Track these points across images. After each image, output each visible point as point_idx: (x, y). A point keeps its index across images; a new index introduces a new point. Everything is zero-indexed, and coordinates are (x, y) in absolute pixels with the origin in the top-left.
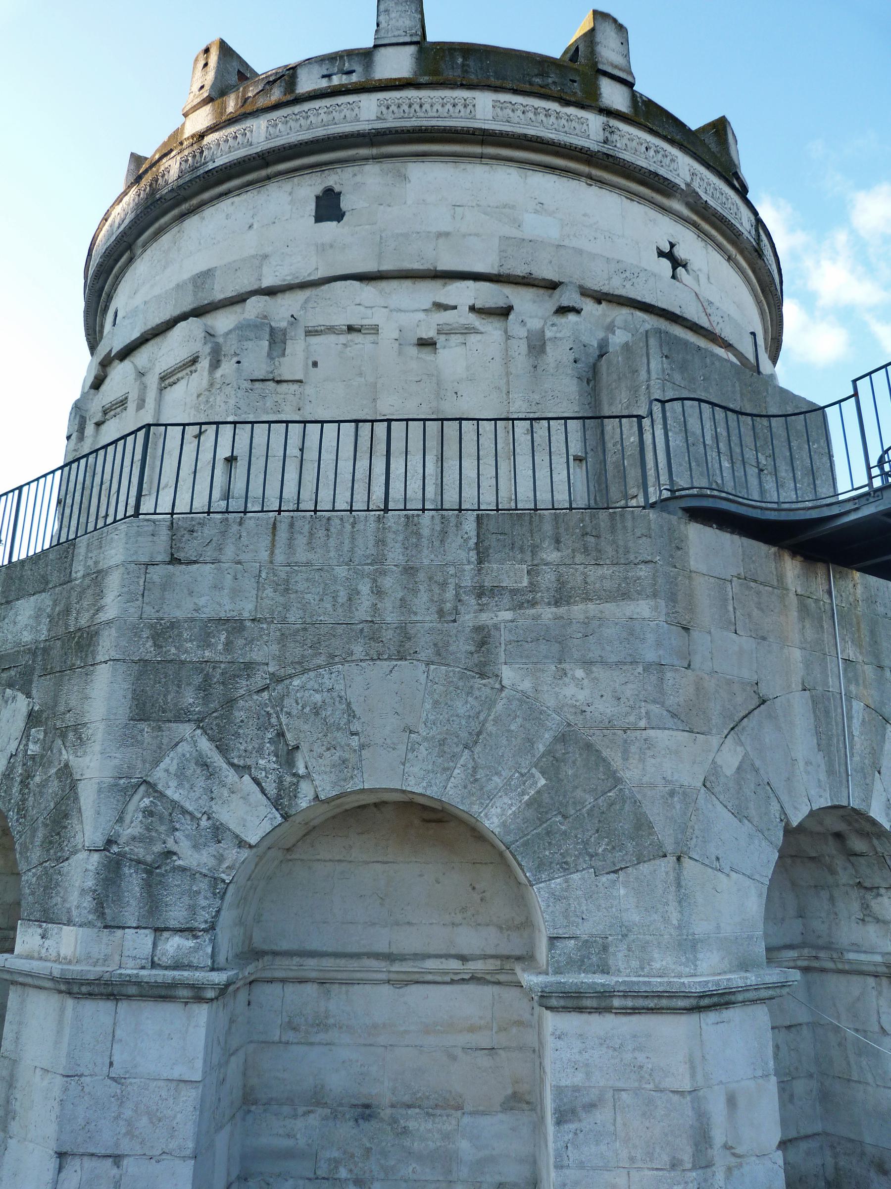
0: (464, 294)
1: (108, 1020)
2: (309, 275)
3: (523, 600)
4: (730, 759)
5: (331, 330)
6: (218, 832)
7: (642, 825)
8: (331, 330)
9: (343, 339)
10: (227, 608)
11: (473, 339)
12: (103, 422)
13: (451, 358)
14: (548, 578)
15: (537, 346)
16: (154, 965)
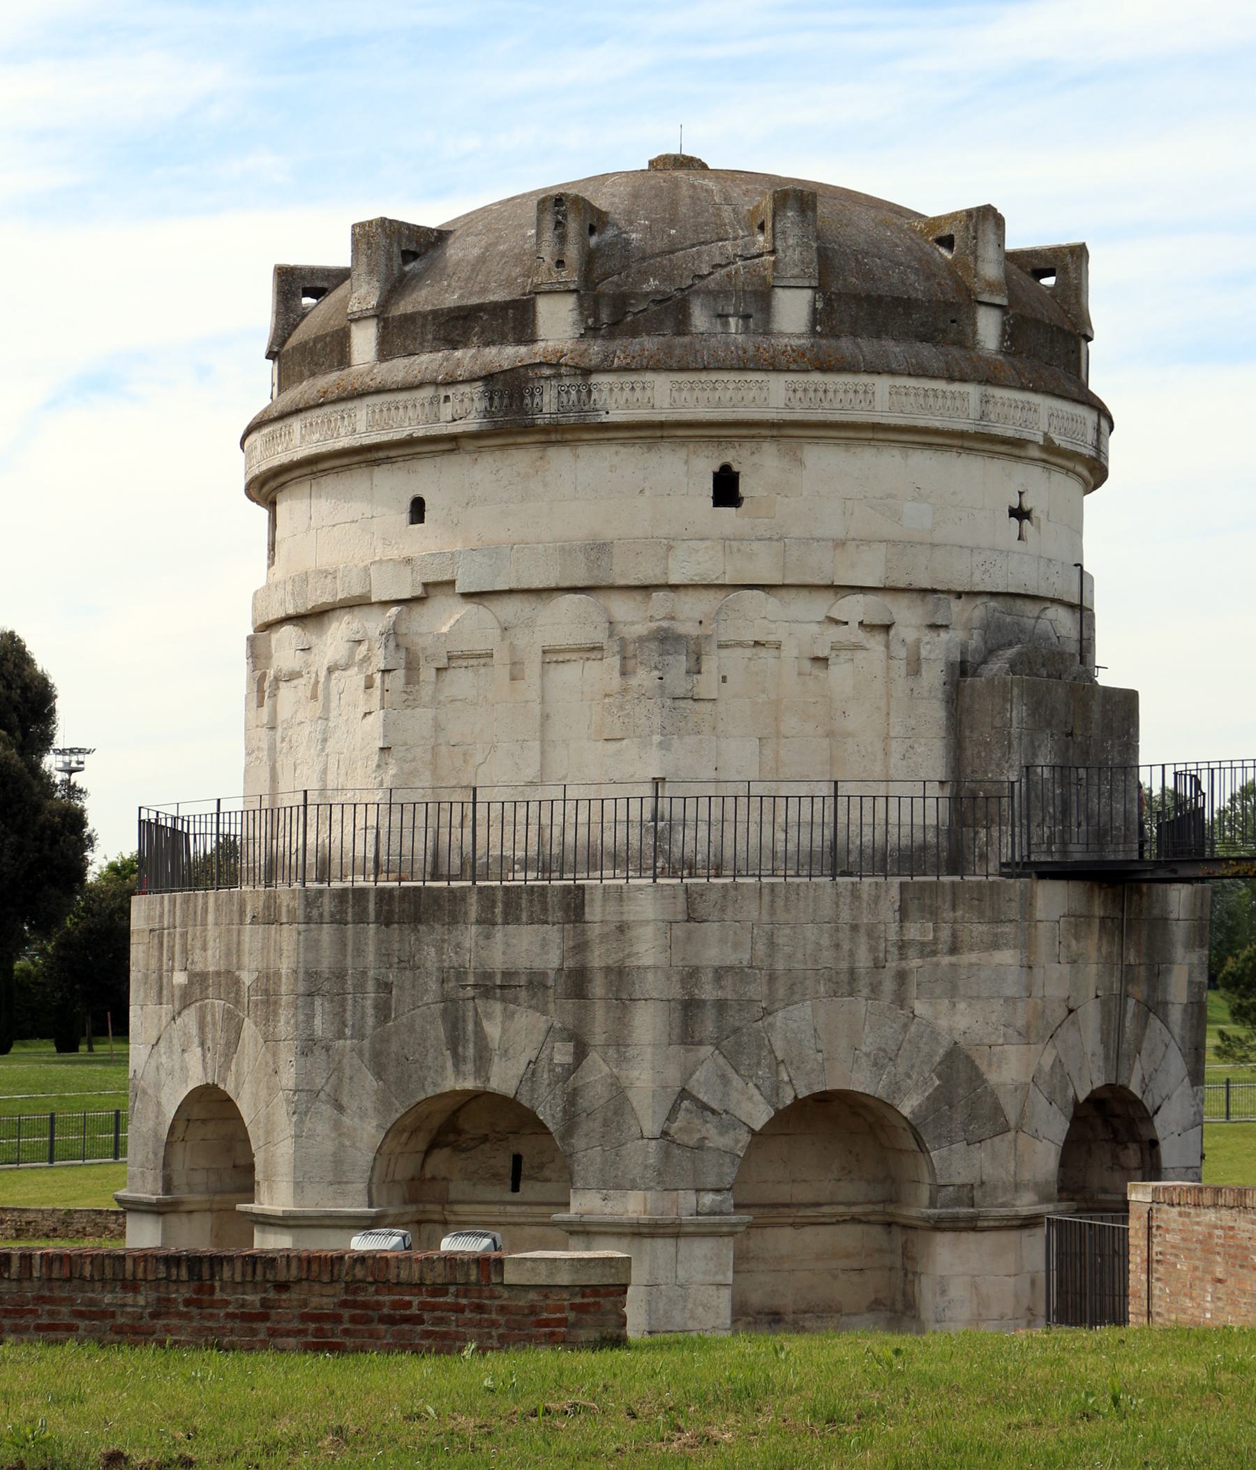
1: (673, 1250)
2: (717, 578)
5: (740, 644)
8: (740, 644)
9: (748, 652)
12: (446, 669)
16: (698, 1214)
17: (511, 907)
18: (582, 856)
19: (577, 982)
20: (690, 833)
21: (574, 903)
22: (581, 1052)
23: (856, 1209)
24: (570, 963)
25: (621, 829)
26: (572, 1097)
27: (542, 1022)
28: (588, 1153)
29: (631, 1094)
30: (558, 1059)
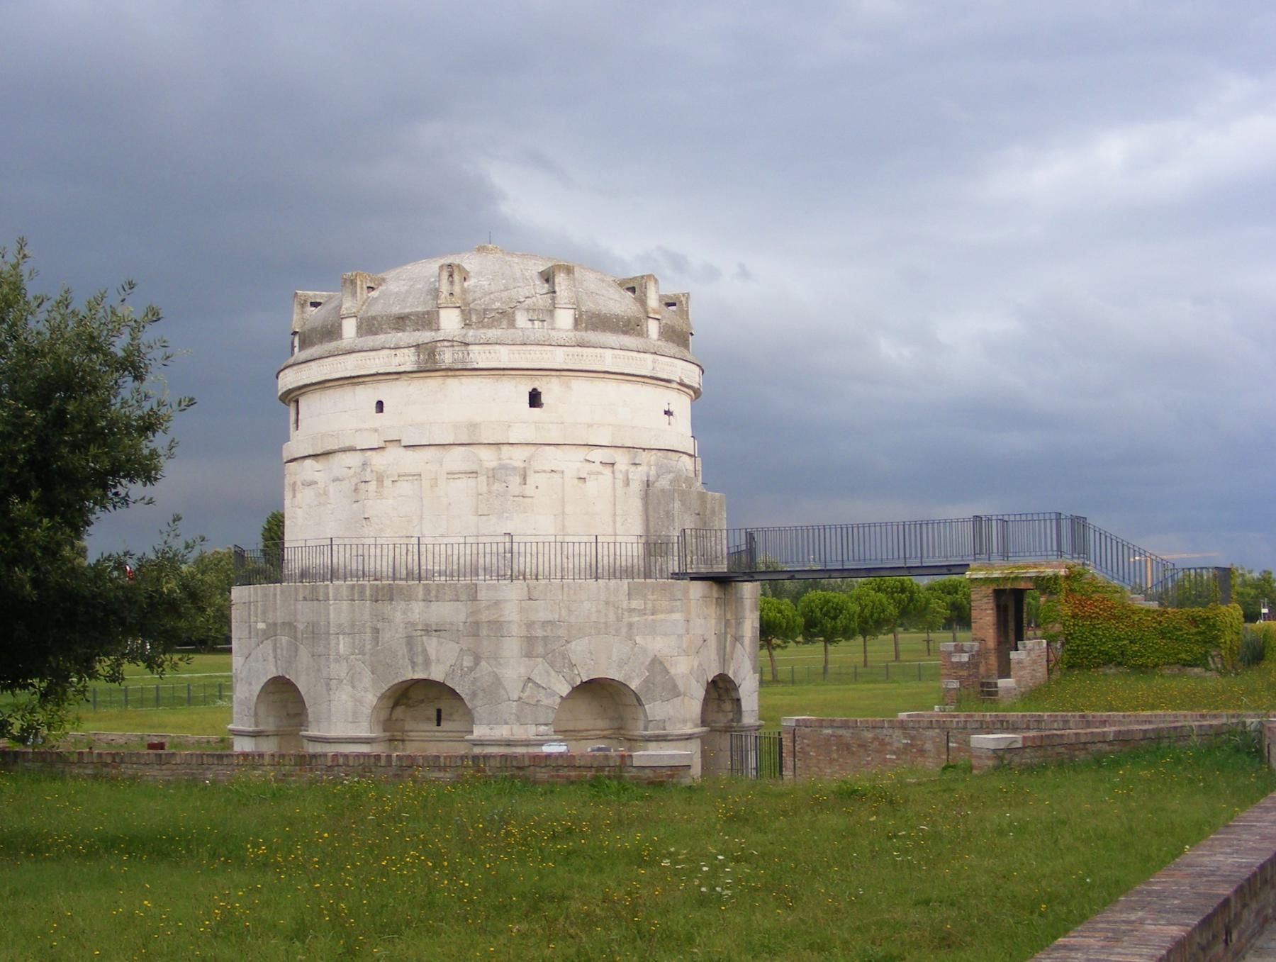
0: (597, 455)
3: (642, 612)
4: (696, 664)
5: (544, 471)
6: (553, 693)
7: (675, 686)
8: (544, 471)
9: (548, 475)
10: (550, 618)
11: (600, 477)
13: (591, 486)
14: (649, 606)
15: (627, 482)
18: (468, 570)
20: (522, 559)
23: (606, 733)
25: (488, 557)
27: (457, 647)
30: (465, 664)
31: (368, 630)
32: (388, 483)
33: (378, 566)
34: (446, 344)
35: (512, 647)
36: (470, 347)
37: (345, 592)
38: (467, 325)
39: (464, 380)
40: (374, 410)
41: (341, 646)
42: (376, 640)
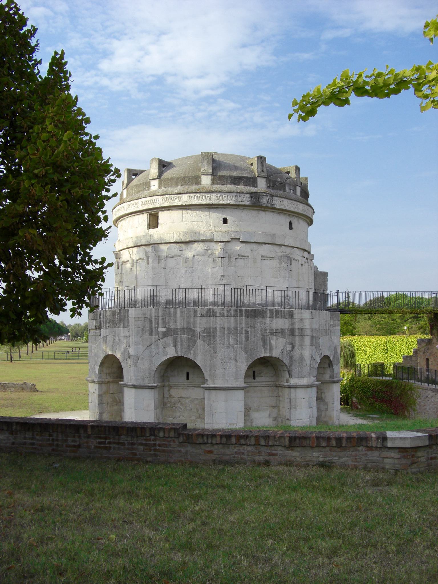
17: (277, 314)
19: (292, 332)
21: (291, 315)
22: (293, 347)
24: (290, 327)
26: (291, 357)
28: (295, 370)
29: (304, 356)
31: (244, 332)
32: (233, 259)
33: (230, 300)
34: (264, 194)
35: (307, 340)
36: (274, 198)
37: (232, 312)
38: (269, 187)
39: (267, 213)
40: (222, 222)
41: (231, 340)
42: (247, 338)
